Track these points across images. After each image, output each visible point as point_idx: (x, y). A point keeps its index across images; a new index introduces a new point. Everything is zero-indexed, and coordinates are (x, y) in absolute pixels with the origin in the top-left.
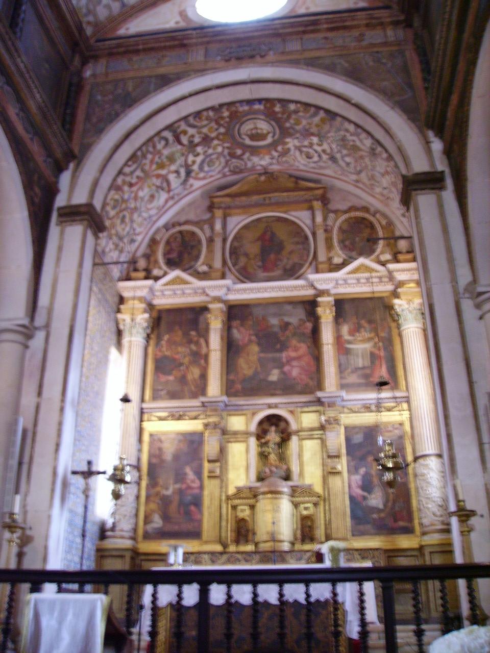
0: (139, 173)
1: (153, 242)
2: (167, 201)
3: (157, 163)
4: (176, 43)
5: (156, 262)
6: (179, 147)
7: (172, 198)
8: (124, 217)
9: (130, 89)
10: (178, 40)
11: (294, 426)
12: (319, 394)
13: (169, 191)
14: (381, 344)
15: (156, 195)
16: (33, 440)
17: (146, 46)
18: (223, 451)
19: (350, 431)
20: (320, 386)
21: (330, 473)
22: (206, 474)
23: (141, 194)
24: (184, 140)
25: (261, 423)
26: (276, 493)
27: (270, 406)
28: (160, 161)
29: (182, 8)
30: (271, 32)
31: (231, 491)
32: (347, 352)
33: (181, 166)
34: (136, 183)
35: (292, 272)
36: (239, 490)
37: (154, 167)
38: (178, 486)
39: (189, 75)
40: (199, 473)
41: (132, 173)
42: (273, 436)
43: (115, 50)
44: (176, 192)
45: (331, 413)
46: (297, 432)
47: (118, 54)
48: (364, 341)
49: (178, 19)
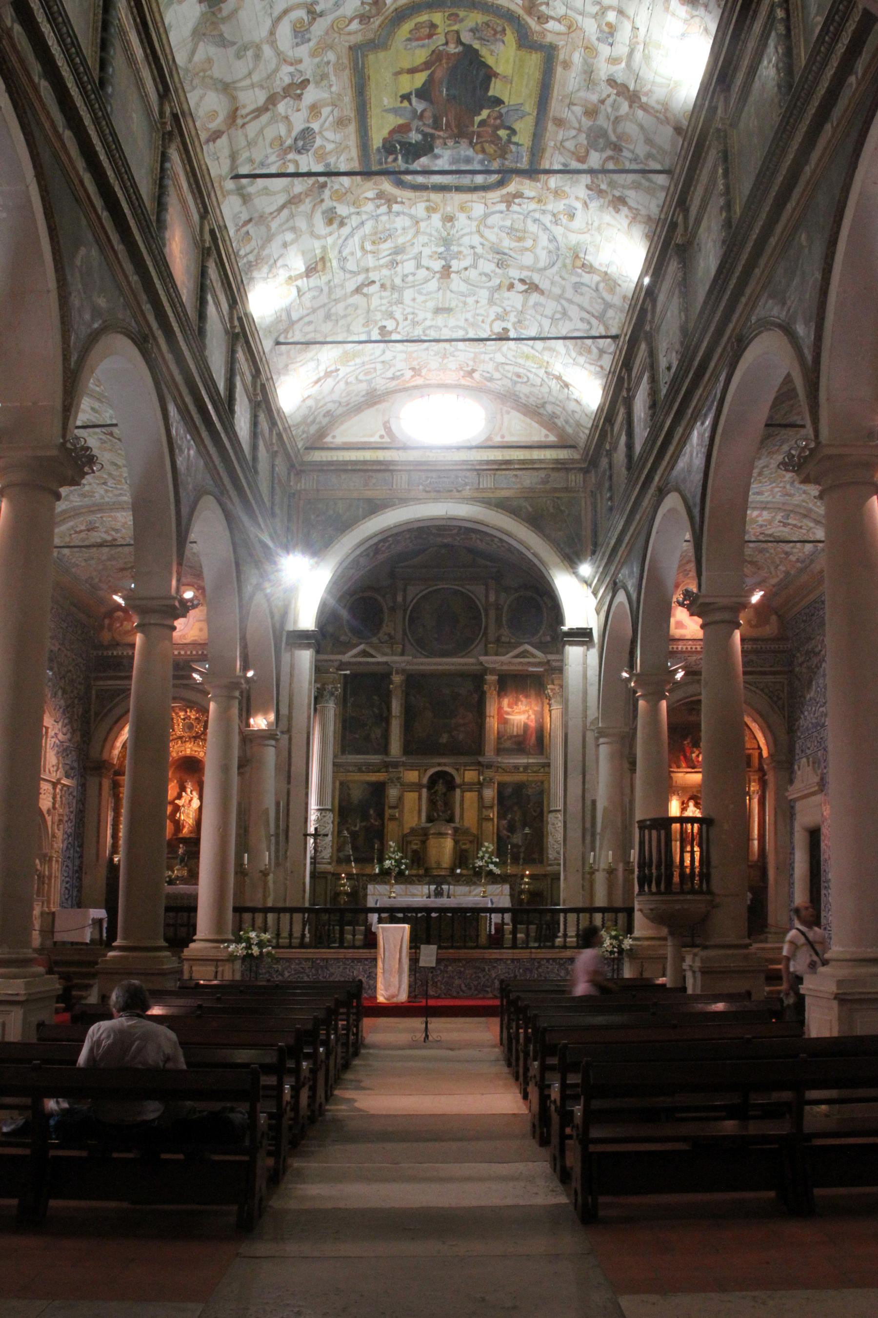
11: (458, 780)
12: (481, 759)
14: (533, 717)
18: (400, 799)
19: (502, 786)
20: (480, 751)
21: (482, 820)
22: (387, 816)
25: (431, 777)
26: (441, 835)
27: (439, 765)
30: (469, 467)
31: (407, 831)
32: (505, 722)
35: (463, 647)
36: (413, 831)
38: (364, 824)
40: (381, 815)
42: (440, 787)
45: (489, 773)
46: (460, 786)
48: (519, 713)
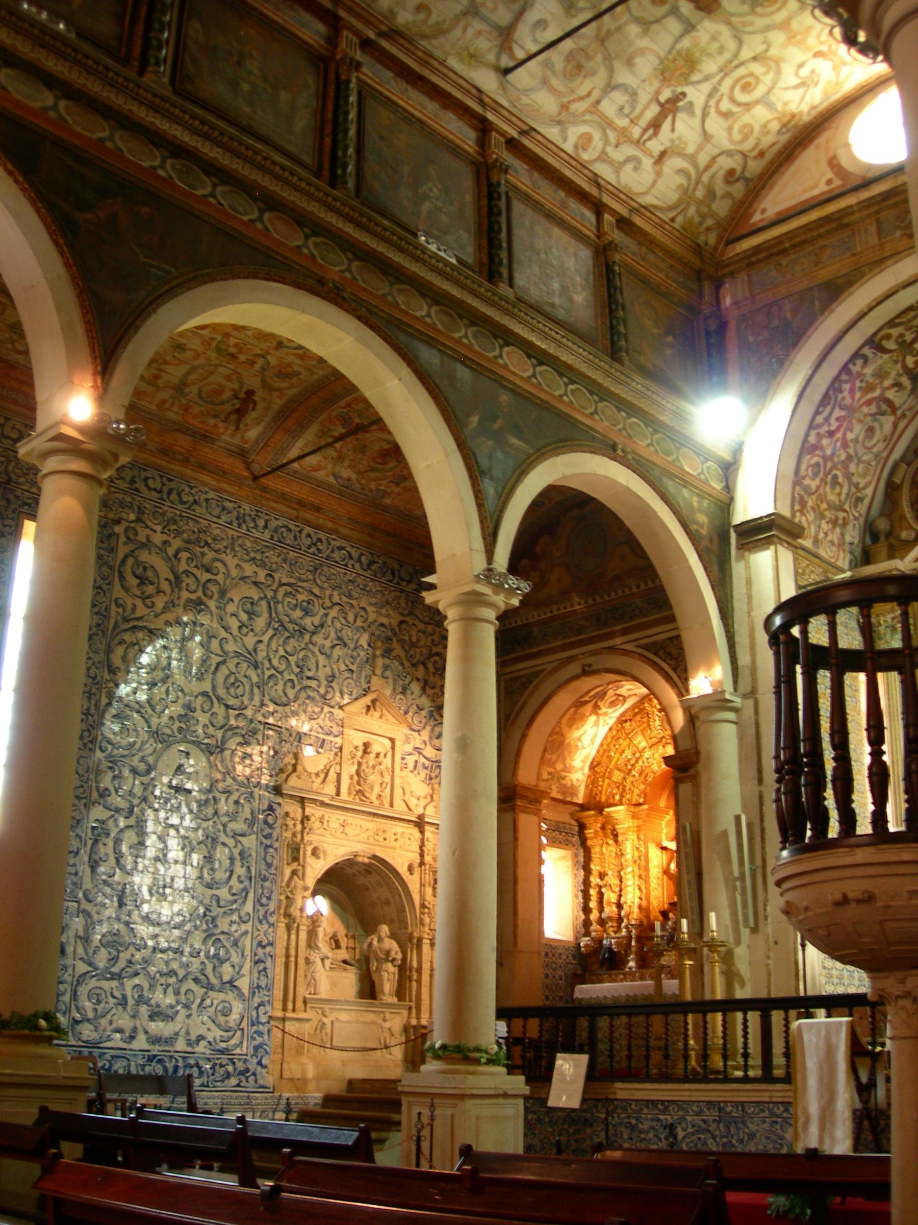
0: (838, 413)
1: (892, 489)
2: (895, 425)
3: (860, 388)
4: (834, 225)
5: (903, 517)
6: (886, 356)
7: (904, 416)
8: (835, 477)
9: (789, 316)
10: (835, 220)
13: (894, 412)
15: (876, 425)
16: (763, 839)
17: (793, 242)
23: (850, 436)
24: (891, 345)
28: (864, 385)
29: (832, 153)
33: (900, 375)
34: (839, 427)
37: (858, 395)
39: (864, 275)
41: (827, 420)
43: (754, 259)
44: (907, 405)
47: (761, 261)
49: (830, 175)
